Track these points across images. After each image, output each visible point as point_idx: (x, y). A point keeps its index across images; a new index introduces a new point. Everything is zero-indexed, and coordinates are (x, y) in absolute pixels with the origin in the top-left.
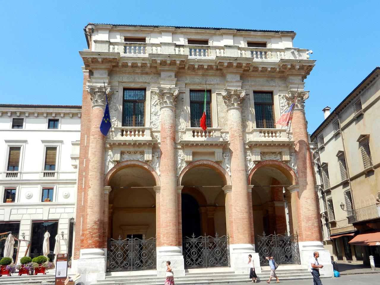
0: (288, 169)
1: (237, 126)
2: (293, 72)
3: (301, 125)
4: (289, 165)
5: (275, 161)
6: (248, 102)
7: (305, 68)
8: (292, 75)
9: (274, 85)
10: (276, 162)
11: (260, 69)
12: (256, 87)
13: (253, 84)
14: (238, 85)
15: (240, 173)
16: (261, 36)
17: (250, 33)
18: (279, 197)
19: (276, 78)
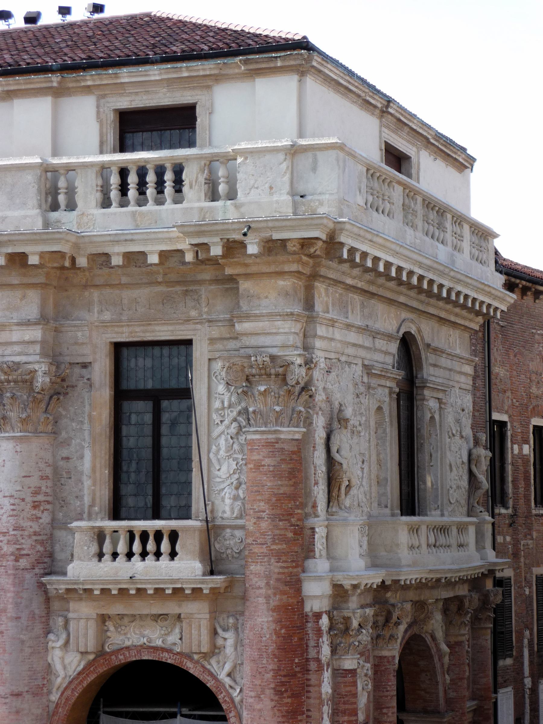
0: (211, 684)
1: (11, 513)
2: (246, 265)
3: (262, 504)
4: (213, 665)
5: (163, 650)
6: (86, 396)
7: (290, 247)
8: (247, 276)
9: (193, 313)
10: (166, 655)
11: (117, 261)
12: (120, 330)
13: (107, 316)
14: (27, 338)
15: (4, 707)
16: (170, 82)
17: (117, 77)
18: (422, 693)
19: (200, 282)
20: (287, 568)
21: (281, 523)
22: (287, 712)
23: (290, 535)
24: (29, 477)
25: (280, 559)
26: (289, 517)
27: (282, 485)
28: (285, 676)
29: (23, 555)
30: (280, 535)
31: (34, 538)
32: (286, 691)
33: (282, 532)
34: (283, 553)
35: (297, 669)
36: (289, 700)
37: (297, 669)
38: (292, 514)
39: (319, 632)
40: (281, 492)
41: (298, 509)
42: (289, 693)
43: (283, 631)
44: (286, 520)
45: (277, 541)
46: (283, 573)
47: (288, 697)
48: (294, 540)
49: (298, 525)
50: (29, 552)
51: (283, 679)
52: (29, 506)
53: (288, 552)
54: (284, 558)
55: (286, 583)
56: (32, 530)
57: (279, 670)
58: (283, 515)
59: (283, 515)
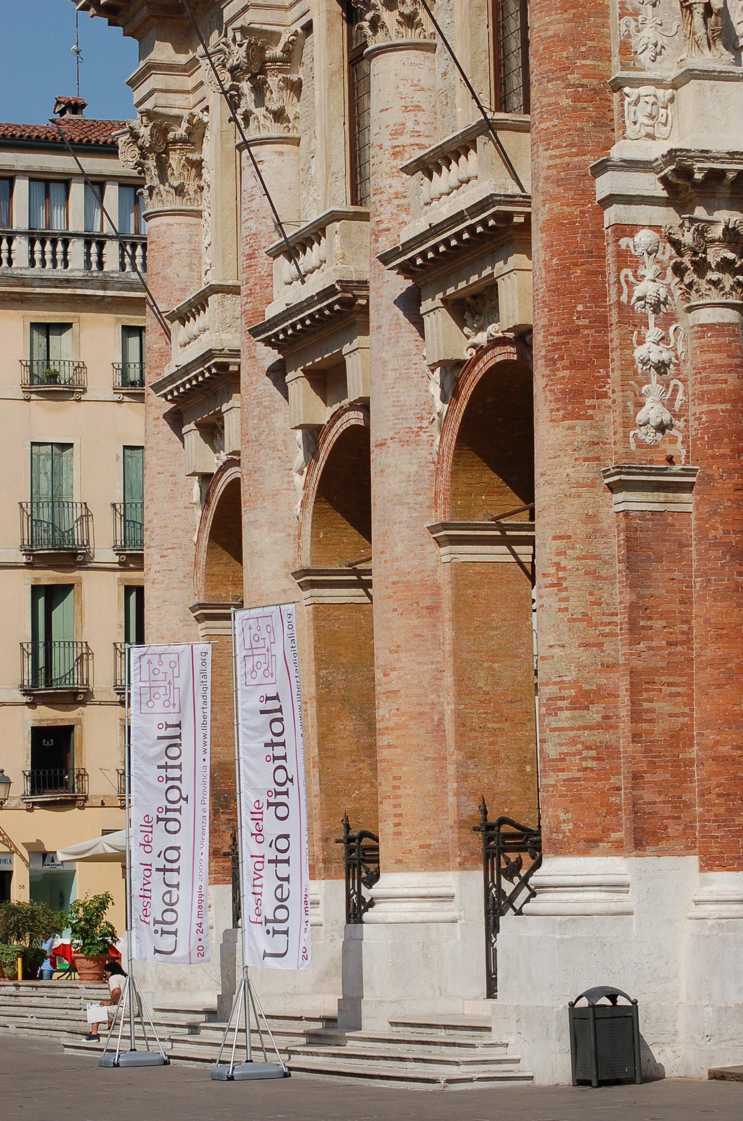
20: (561, 156)
21: (550, 85)
22: (563, 392)
23: (565, 102)
24: (387, 109)
25: (549, 144)
26: (563, 73)
27: (550, 23)
28: (558, 334)
29: (382, 231)
30: (550, 105)
31: (396, 202)
32: (561, 358)
33: (552, 99)
34: (555, 133)
35: (581, 322)
36: (566, 373)
37: (581, 322)
38: (569, 68)
39: (624, 258)
40: (551, 33)
41: (585, 58)
42: (566, 362)
43: (555, 261)
44: (557, 79)
45: (545, 116)
46: (555, 166)
47: (565, 368)
48: (574, 111)
49: (582, 86)
50: (390, 226)
51: (556, 340)
52: (388, 156)
53: (562, 132)
54: (555, 142)
55: (558, 182)
56: (392, 191)
57: (551, 325)
58: (553, 72)
59: (553, 72)
